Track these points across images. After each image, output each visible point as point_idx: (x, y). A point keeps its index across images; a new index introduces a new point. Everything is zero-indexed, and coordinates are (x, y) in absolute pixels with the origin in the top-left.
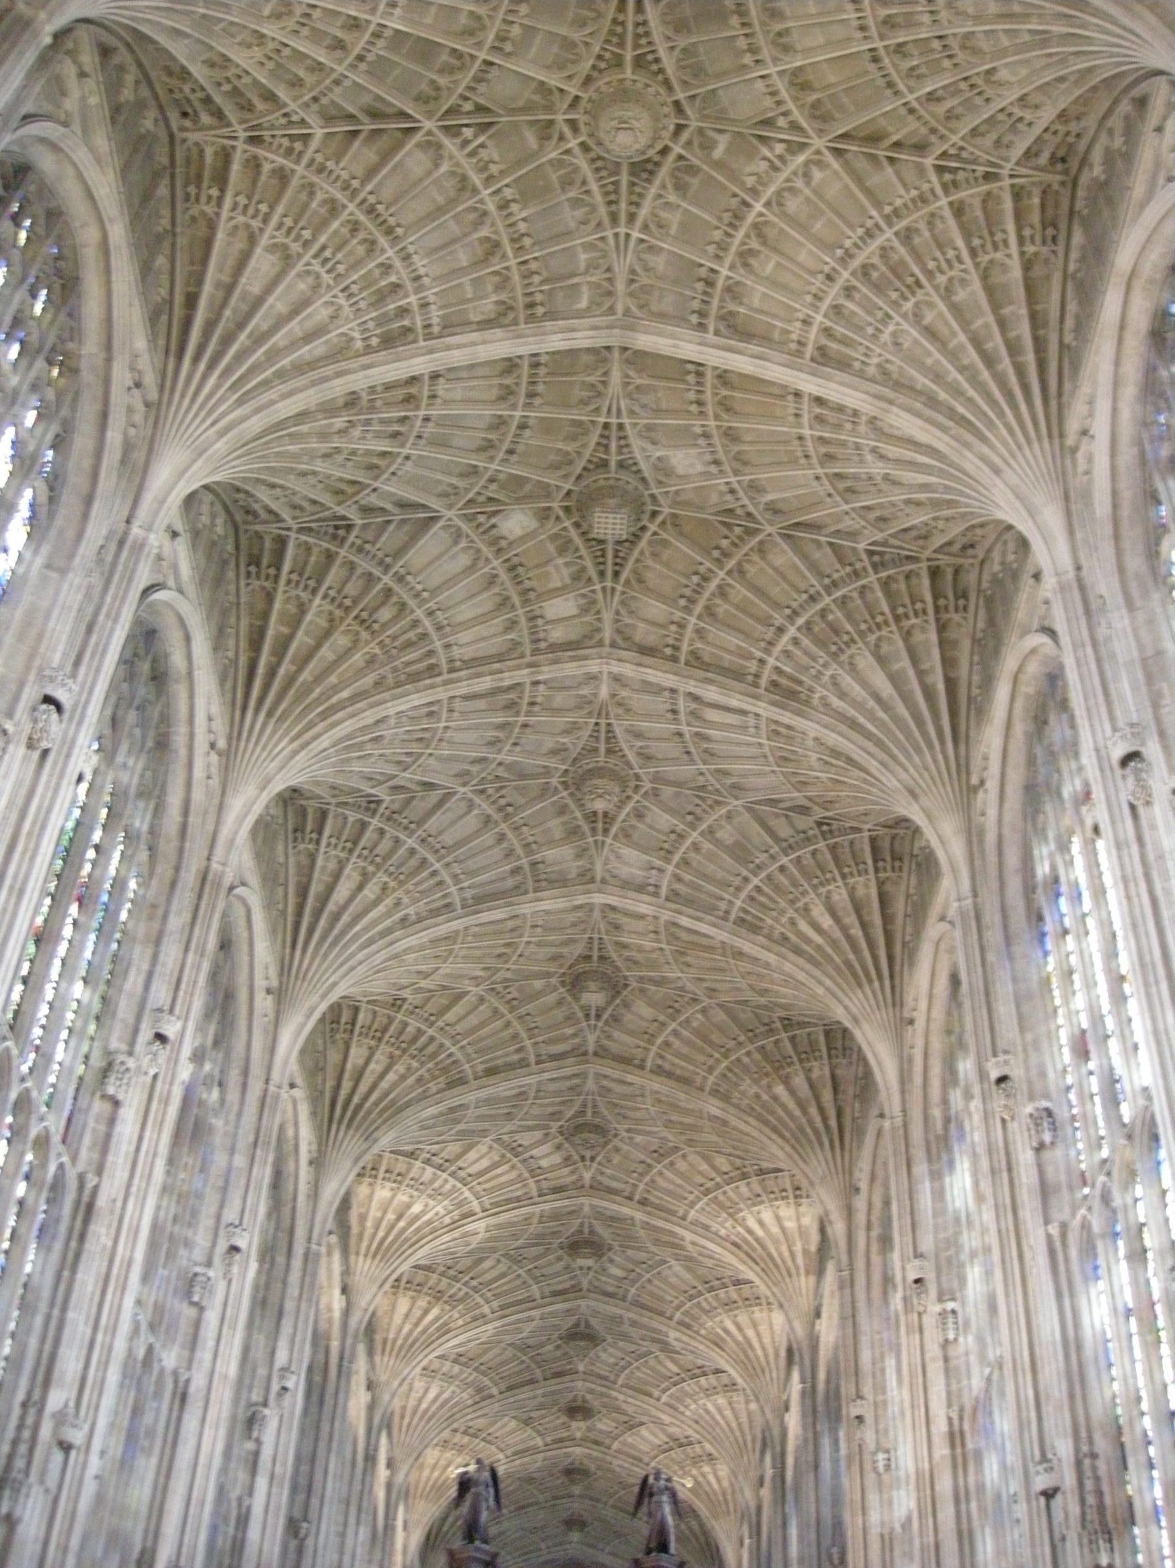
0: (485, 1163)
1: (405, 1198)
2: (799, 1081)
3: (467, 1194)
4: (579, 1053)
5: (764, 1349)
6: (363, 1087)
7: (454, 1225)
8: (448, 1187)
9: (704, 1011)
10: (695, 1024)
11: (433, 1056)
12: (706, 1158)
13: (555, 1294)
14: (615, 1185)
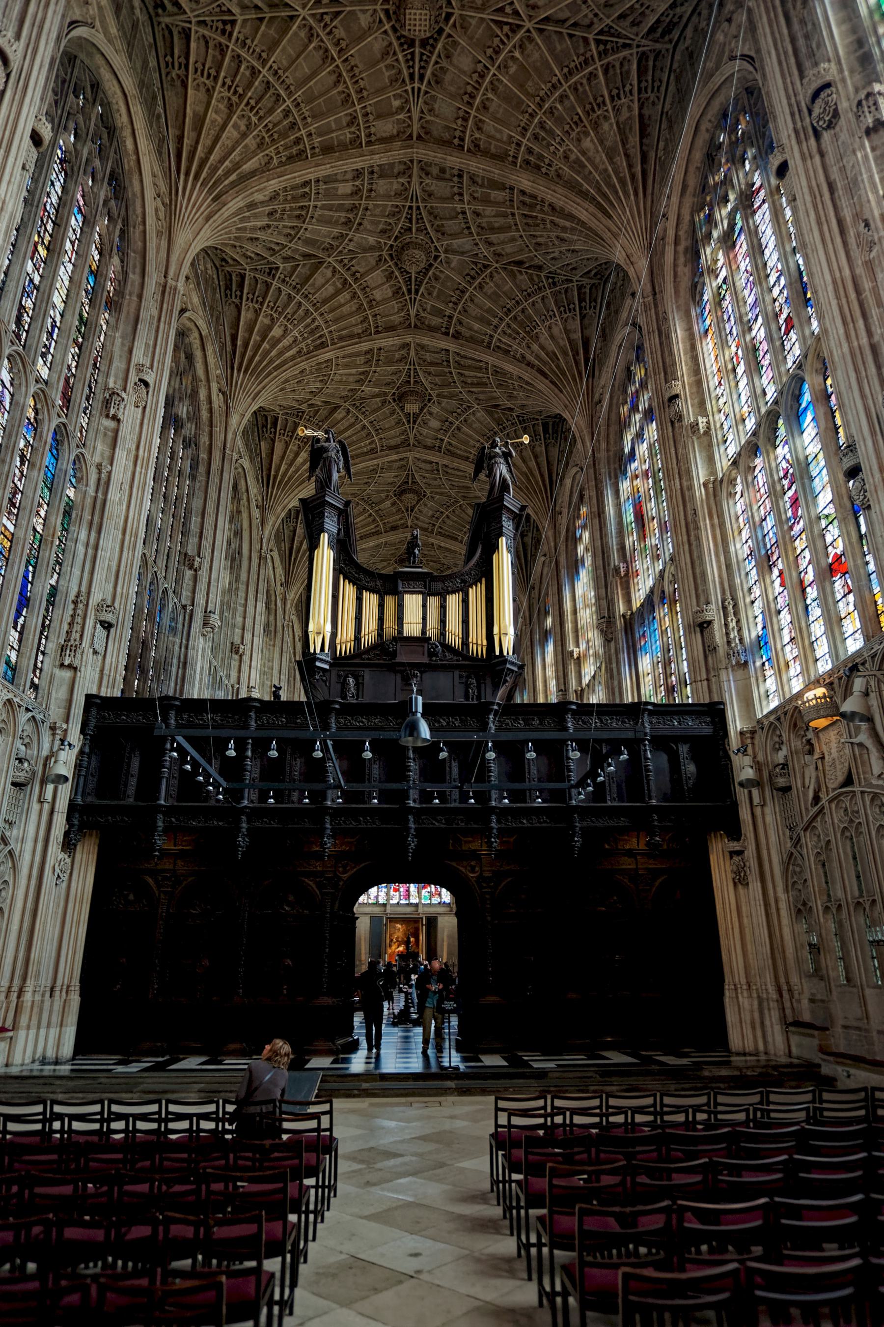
0: (329, 289)
1: (267, 321)
2: (609, 128)
3: (320, 321)
4: (404, 136)
5: (542, 476)
6: (205, 141)
7: (308, 354)
8: (301, 312)
9: (522, 47)
10: (513, 69)
11: (271, 111)
12: (512, 275)
13: (391, 448)
14: (436, 321)
